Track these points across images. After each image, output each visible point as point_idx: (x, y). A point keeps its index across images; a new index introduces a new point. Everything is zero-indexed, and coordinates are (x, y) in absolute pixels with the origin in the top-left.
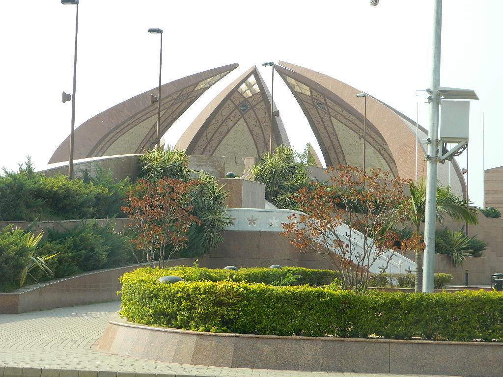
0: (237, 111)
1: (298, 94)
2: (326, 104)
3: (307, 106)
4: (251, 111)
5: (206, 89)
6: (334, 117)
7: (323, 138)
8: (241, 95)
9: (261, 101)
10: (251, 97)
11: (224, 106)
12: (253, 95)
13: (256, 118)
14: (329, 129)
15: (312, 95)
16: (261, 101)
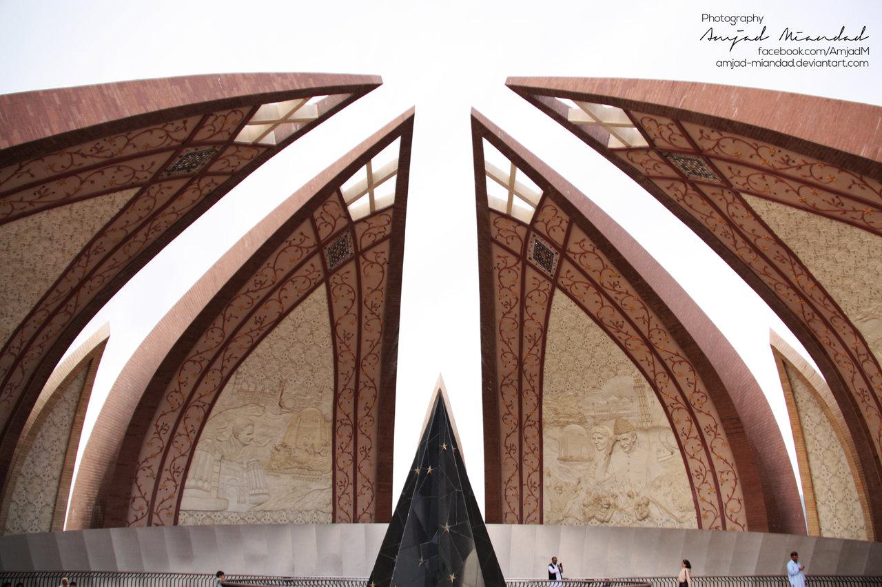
0: (316, 260)
1: (493, 217)
2: (563, 251)
3: (496, 261)
4: (351, 267)
5: (271, 151)
6: (565, 291)
7: (499, 353)
8: (344, 206)
9: (384, 239)
10: (364, 220)
11: (290, 238)
12: (374, 214)
13: (354, 285)
14: (532, 328)
15: (531, 227)
16: (384, 239)
